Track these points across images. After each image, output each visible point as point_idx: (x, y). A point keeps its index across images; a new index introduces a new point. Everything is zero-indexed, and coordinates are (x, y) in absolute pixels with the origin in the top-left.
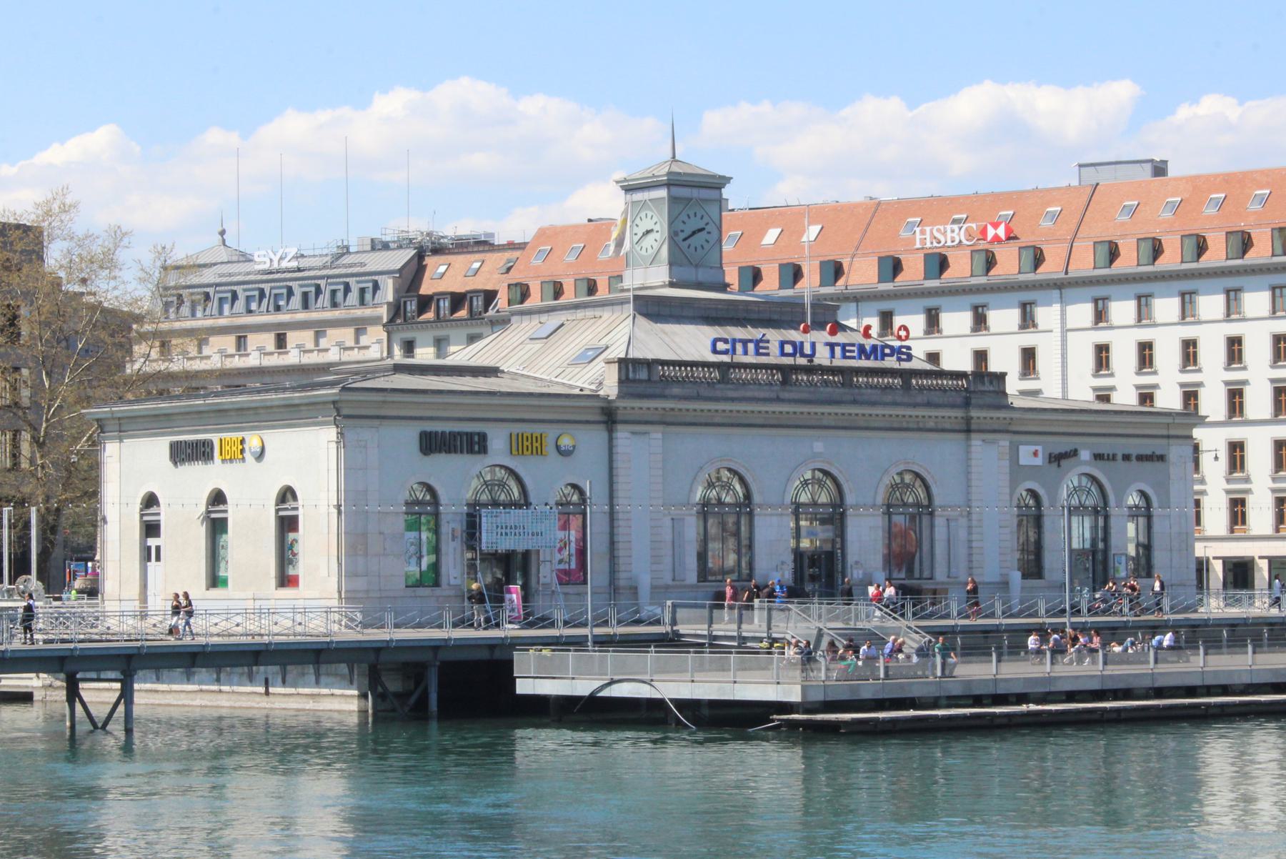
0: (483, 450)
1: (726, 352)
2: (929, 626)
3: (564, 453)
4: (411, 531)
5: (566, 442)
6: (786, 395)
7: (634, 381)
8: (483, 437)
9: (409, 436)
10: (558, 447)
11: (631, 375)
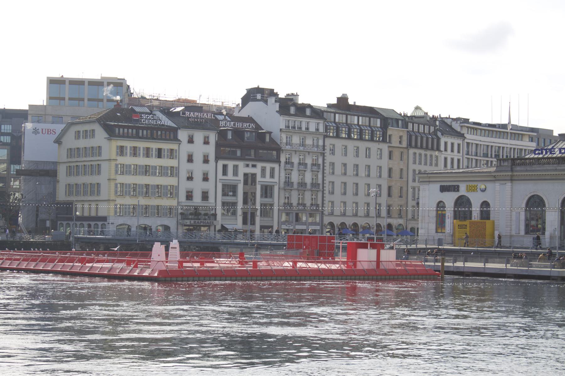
0: (458, 191)
1: (539, 154)
2: (527, 251)
3: (483, 191)
4: (490, 217)
5: (483, 187)
6: (559, 168)
7: (503, 166)
8: (458, 186)
9: (437, 186)
10: (480, 189)
11: (502, 164)
